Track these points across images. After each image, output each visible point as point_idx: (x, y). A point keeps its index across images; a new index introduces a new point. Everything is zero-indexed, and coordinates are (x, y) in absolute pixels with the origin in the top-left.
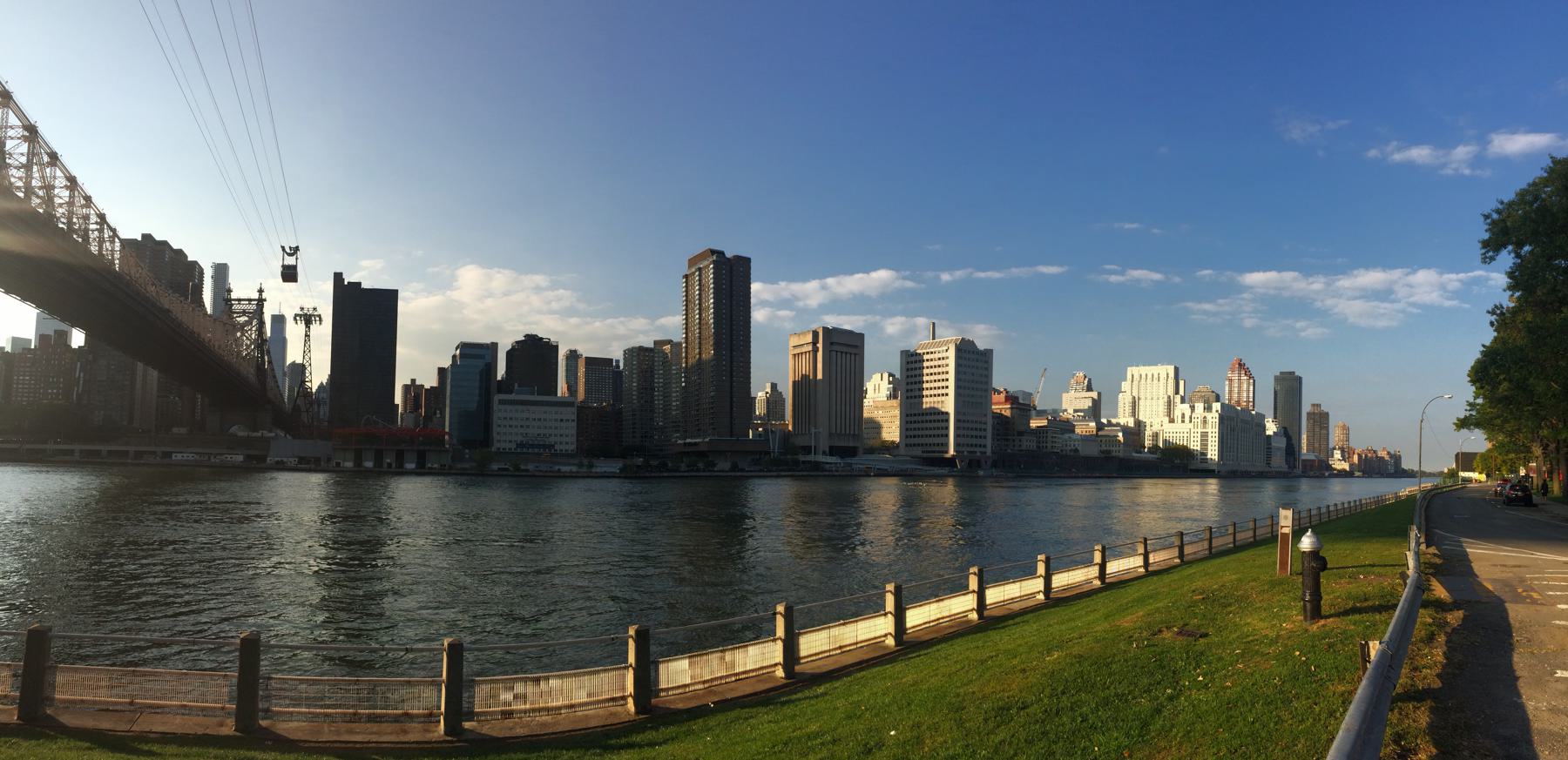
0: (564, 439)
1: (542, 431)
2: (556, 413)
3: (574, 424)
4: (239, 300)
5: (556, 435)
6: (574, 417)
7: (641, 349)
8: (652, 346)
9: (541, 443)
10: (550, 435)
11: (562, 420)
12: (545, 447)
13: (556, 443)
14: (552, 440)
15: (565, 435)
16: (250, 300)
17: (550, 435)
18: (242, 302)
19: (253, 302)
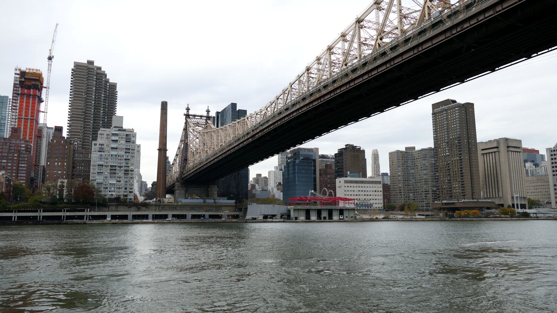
0: (377, 201)
1: (366, 197)
2: (373, 187)
3: (382, 193)
4: (195, 116)
5: (373, 199)
6: (381, 189)
7: (398, 152)
8: (404, 150)
9: (367, 204)
10: (370, 199)
11: (375, 191)
12: (367, 205)
13: (373, 203)
14: (372, 202)
15: (378, 201)
16: (201, 116)
17: (370, 199)
18: (196, 117)
19: (203, 118)
